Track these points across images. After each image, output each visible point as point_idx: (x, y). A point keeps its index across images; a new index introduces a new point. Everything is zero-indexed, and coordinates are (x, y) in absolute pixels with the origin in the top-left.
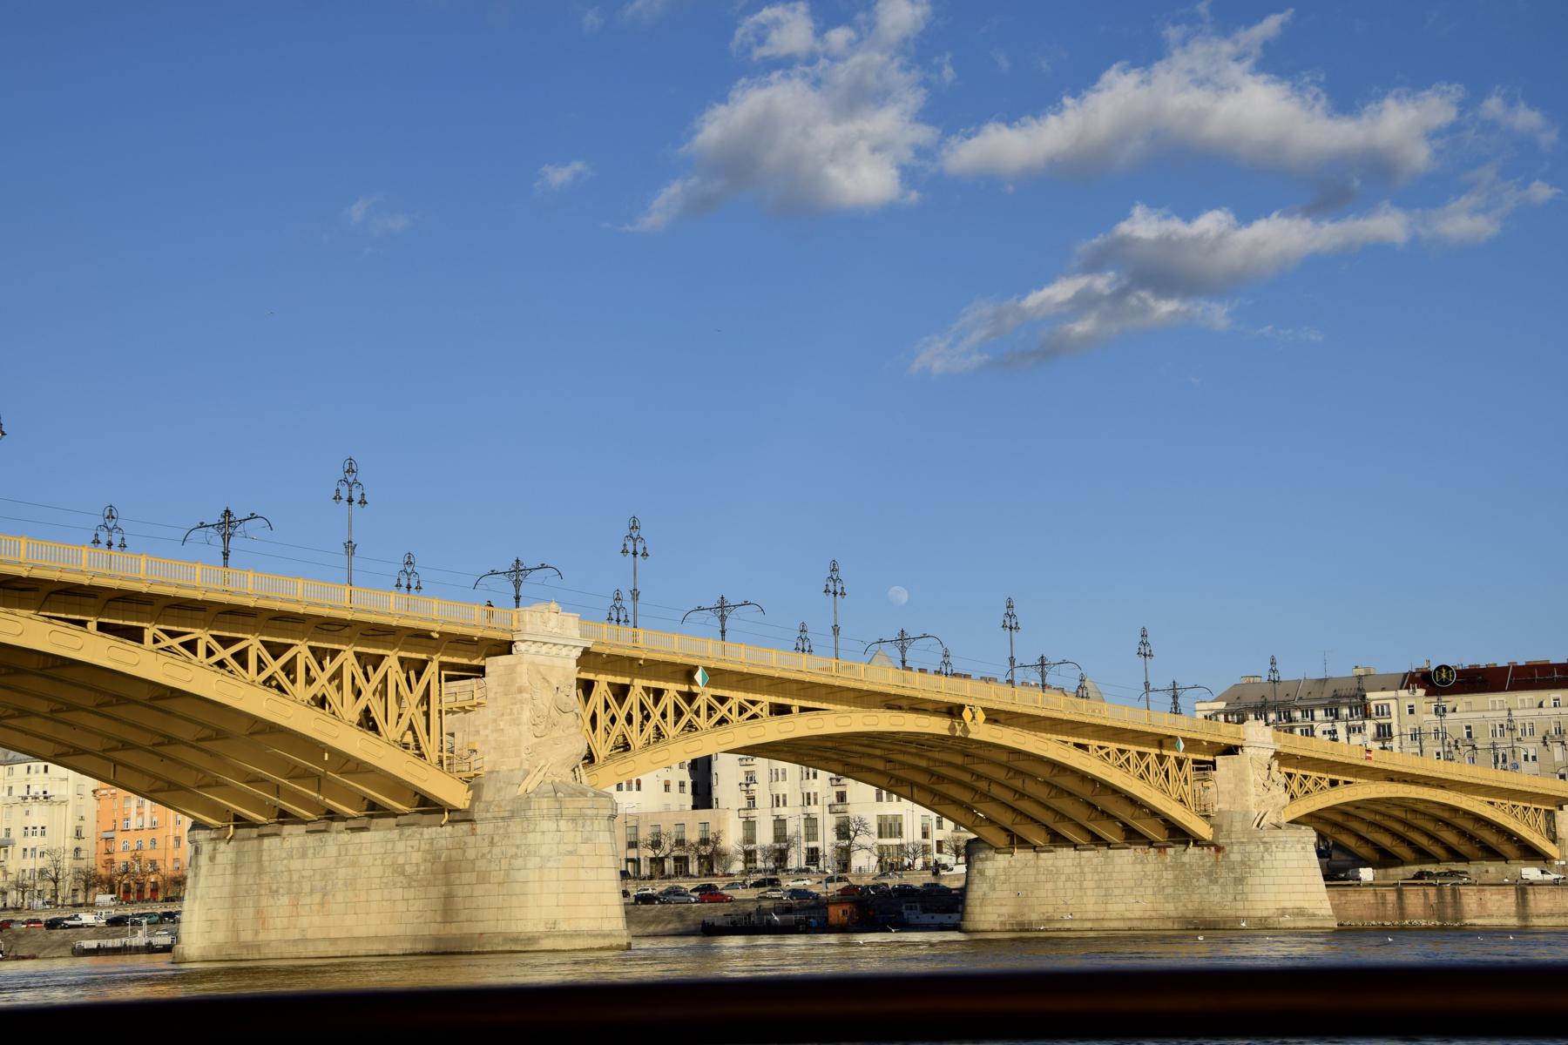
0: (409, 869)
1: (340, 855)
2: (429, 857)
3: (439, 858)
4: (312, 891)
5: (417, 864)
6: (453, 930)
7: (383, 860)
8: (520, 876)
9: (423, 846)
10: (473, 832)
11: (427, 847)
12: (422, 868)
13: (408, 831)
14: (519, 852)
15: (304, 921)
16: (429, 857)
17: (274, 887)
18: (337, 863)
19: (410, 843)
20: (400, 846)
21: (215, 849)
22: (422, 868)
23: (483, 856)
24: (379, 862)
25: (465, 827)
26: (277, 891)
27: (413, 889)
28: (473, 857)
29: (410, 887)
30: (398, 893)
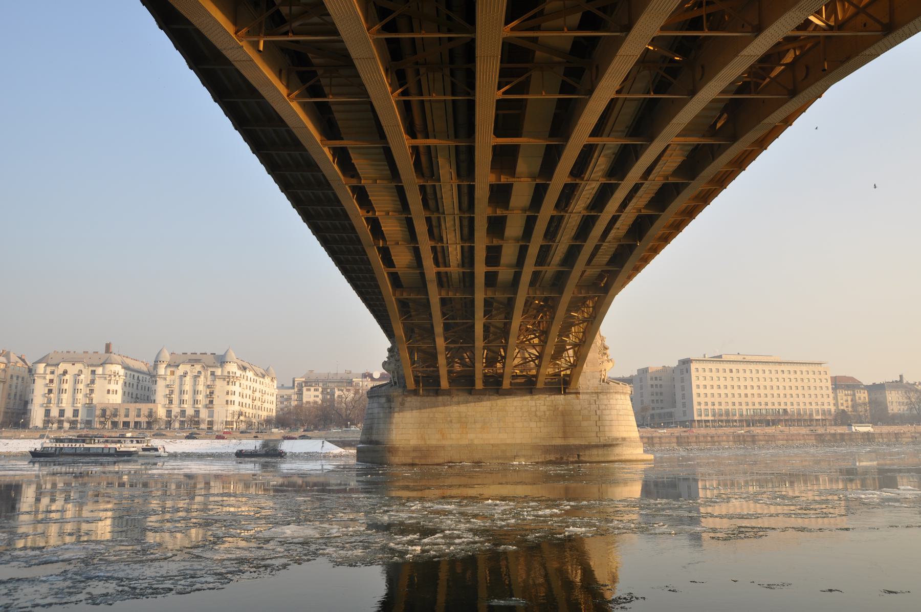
0: (538, 413)
1: (492, 406)
2: (551, 408)
3: (558, 409)
4: (475, 422)
5: (544, 412)
6: (573, 442)
7: (521, 409)
8: (607, 418)
9: (547, 404)
10: (578, 398)
11: (549, 404)
12: (547, 413)
13: (536, 397)
14: (606, 408)
15: (471, 436)
16: (551, 408)
17: (449, 419)
18: (491, 409)
19: (537, 402)
20: (532, 403)
21: (403, 400)
22: (547, 413)
23: (585, 409)
24: (519, 410)
25: (573, 396)
26: (451, 421)
27: (542, 423)
28: (579, 409)
29: (540, 421)
30: (533, 425)
